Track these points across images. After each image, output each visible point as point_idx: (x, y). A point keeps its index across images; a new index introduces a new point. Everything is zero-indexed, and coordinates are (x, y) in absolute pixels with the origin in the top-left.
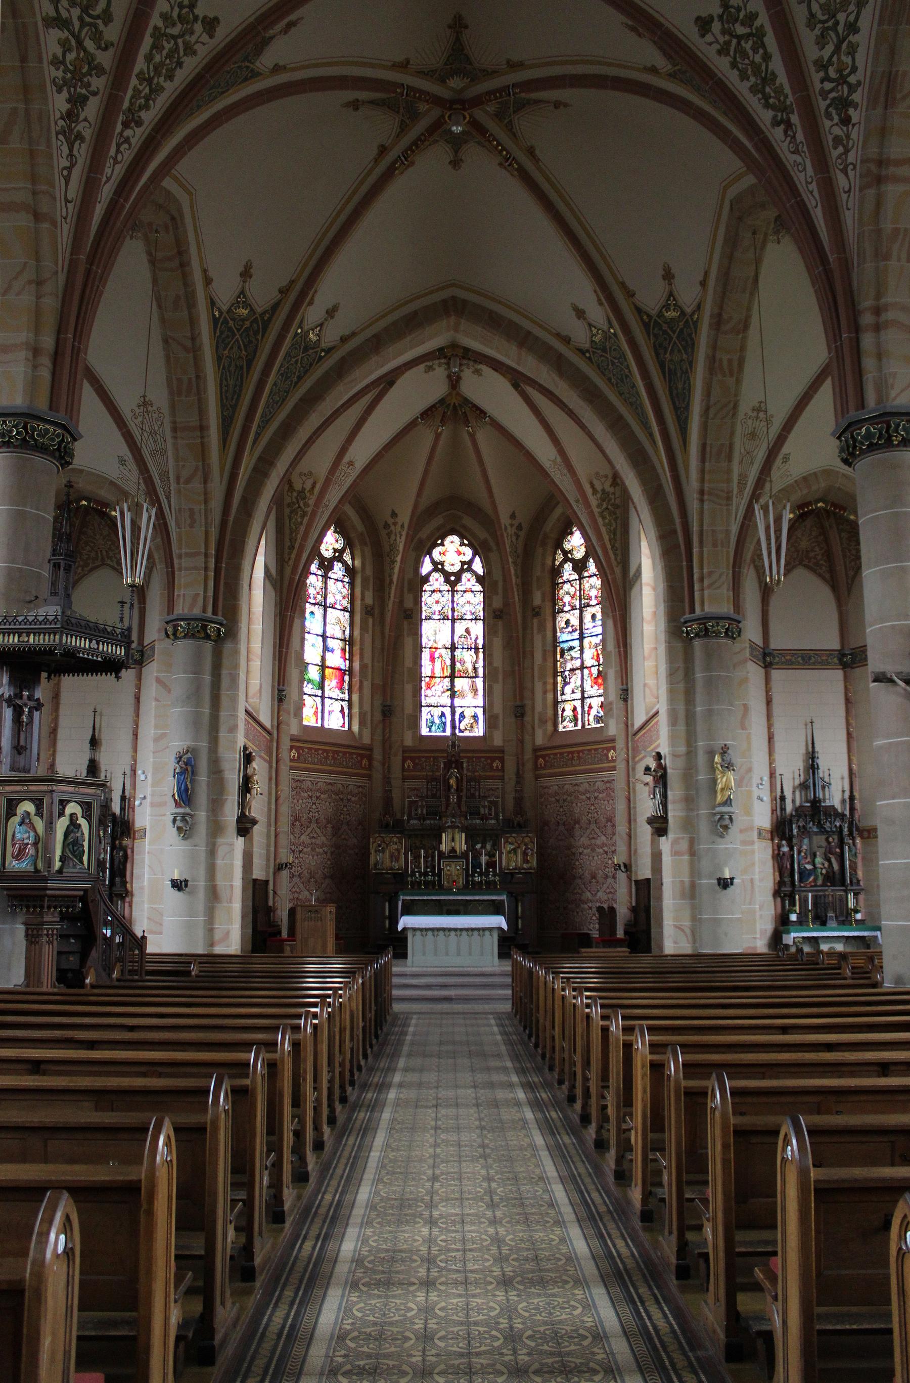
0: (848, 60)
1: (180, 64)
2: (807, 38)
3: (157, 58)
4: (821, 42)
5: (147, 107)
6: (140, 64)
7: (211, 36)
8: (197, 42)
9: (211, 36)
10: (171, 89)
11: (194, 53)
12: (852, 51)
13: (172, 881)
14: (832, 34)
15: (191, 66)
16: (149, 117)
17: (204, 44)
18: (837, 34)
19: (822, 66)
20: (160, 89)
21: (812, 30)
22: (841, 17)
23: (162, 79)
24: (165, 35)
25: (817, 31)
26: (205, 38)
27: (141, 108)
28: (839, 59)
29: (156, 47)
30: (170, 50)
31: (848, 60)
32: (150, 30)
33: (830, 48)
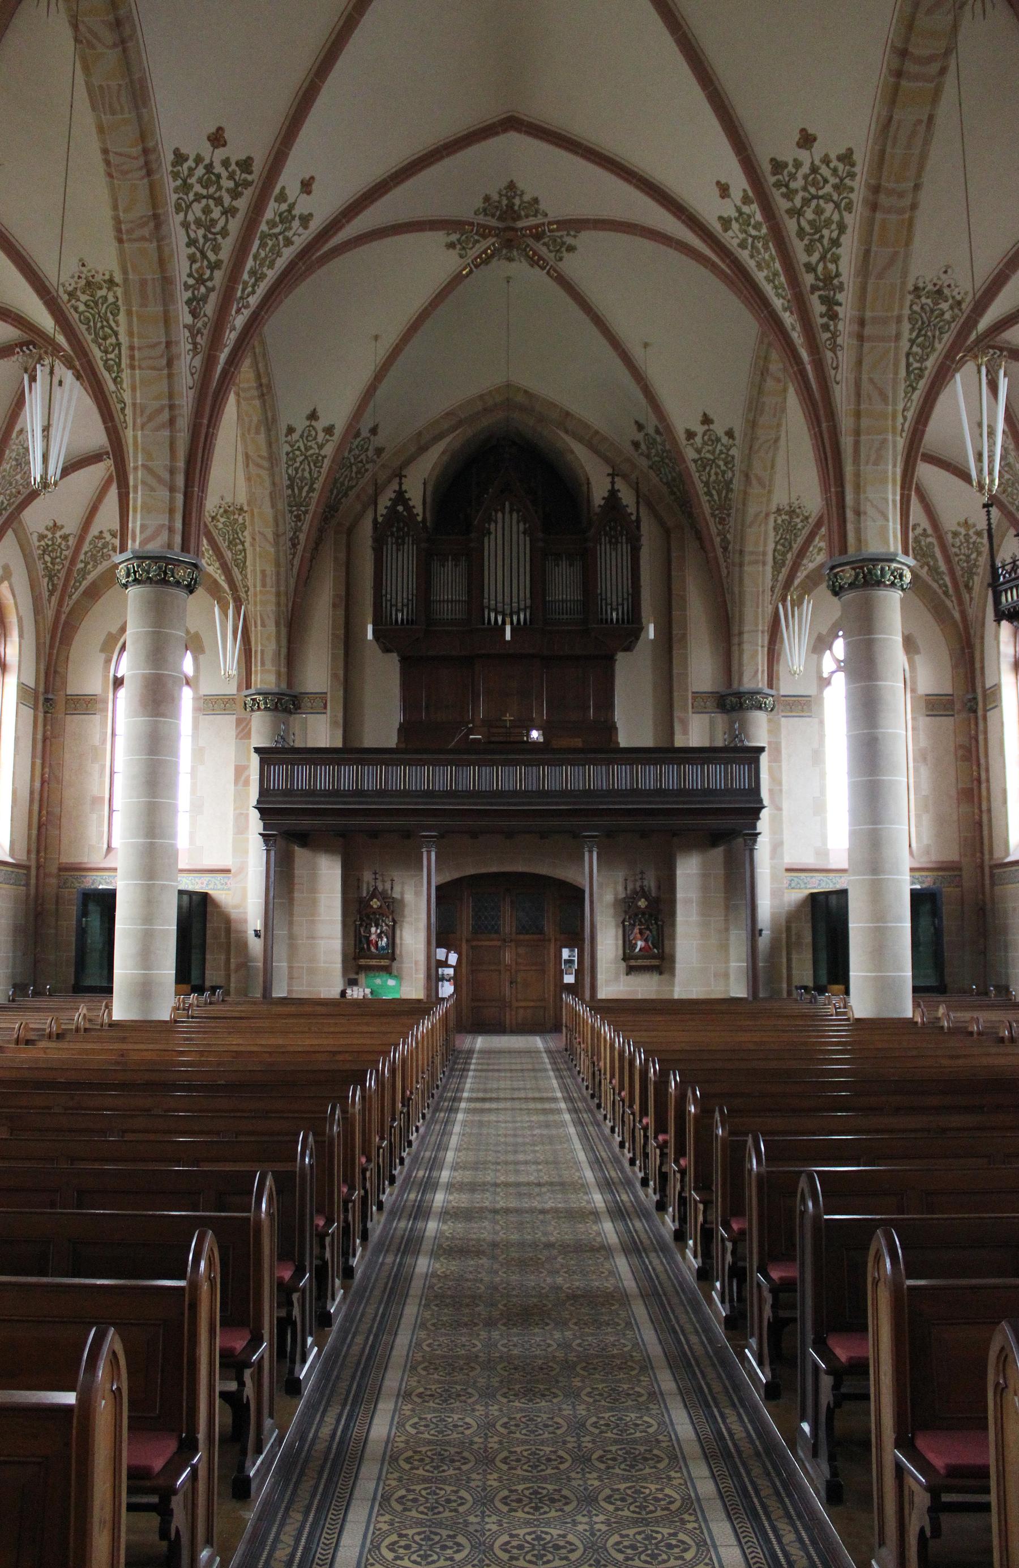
0: (832, 267)
1: (279, 254)
2: (798, 247)
3: (263, 254)
4: (809, 250)
5: (253, 292)
6: (250, 263)
7: (306, 228)
8: (294, 235)
9: (306, 228)
10: (271, 275)
11: (292, 243)
12: (836, 260)
13: (256, 931)
14: (818, 245)
15: (288, 254)
16: (253, 301)
17: (299, 235)
18: (823, 246)
19: (810, 268)
20: (264, 276)
21: (802, 240)
22: (826, 232)
23: (265, 269)
24: (270, 235)
25: (806, 242)
26: (301, 230)
27: (248, 296)
28: (825, 264)
29: (263, 245)
30: (273, 245)
31: (832, 267)
32: (258, 235)
33: (816, 256)
